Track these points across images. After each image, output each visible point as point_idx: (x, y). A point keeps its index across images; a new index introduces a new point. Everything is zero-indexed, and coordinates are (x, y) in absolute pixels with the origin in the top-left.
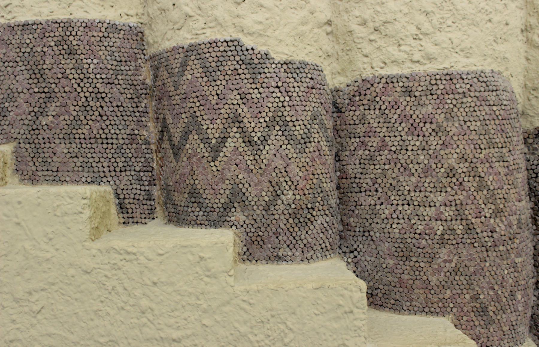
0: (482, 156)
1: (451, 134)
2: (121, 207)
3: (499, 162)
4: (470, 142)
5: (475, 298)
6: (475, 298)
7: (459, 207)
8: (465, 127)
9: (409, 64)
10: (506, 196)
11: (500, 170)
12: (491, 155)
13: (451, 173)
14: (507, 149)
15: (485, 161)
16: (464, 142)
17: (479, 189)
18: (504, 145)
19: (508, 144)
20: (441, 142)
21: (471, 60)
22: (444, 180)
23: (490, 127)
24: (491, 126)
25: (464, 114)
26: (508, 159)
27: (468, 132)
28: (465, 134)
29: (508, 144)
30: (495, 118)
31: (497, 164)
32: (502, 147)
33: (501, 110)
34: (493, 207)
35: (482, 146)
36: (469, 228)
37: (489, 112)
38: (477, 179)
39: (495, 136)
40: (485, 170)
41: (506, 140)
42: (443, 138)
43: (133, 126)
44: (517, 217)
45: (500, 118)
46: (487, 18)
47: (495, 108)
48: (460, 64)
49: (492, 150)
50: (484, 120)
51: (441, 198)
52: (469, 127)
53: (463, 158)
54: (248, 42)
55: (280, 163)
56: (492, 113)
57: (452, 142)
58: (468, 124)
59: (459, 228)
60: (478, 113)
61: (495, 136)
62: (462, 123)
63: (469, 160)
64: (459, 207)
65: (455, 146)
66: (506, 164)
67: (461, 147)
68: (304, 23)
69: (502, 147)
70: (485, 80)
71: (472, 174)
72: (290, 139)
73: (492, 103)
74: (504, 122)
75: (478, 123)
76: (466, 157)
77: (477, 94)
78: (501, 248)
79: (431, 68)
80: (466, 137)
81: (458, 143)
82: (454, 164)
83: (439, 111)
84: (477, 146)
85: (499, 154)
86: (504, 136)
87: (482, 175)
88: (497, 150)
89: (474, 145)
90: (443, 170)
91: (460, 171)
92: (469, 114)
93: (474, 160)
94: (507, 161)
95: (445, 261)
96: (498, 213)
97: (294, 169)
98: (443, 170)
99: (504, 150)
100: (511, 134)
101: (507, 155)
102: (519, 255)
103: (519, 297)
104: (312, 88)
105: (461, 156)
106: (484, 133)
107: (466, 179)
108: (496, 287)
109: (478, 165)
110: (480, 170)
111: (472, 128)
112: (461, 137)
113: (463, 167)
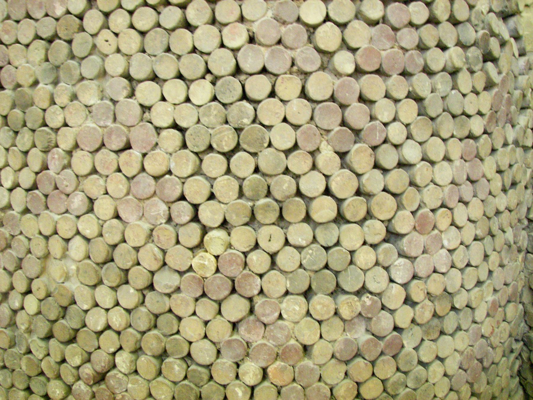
0: (204, 262)
1: (66, 140)
3: (308, 294)
4: (145, 184)
8: (130, 110)
11: (308, 334)
12: (258, 261)
14: (376, 230)
15: (219, 288)
16: (117, 185)
18: (355, 208)
19: (385, 206)
20: (26, 178)
22: (38, 348)
23: (270, 111)
24: (283, 114)
25: (131, 42)
26: (376, 281)
27: (141, 135)
28: (128, 147)
29: (385, 206)
30: (309, 60)
31: (294, 306)
32: (340, 219)
33: (358, 25)
35: (210, 214)
37: (267, 33)
38: (175, 368)
39: (299, 163)
40: (220, 330)
41: (374, 181)
42: (35, 159)
45: (345, 62)
49: (271, 237)
50: (238, 71)
52: (145, 108)
56: (293, 33)
57: (67, 180)
58: (147, 92)
60: (206, 37)
61: (299, 163)
62: (118, 87)
63: (139, 278)
65: (78, 202)
66: (348, 306)
67: (104, 207)
69: (340, 219)
71: (152, 342)
74: (373, 86)
75: (202, 91)
76: (123, 257)
80: (131, 161)
81: (94, 186)
82: (74, 286)
83: (26, 32)
84: (183, 212)
85: (314, 256)
87: (203, 352)
88: (300, 234)
89: (169, 204)
90: (31, 304)
91: (96, 320)
92: (156, 41)
93: (165, 281)
94: (362, 291)
98: (31, 304)
99: (352, 236)
100: (412, 153)
101: (366, 257)
105: (100, 252)
106: (228, 146)
107: (123, 361)
109: (182, 304)
110: (191, 329)
111: (162, 115)
112: (106, 159)
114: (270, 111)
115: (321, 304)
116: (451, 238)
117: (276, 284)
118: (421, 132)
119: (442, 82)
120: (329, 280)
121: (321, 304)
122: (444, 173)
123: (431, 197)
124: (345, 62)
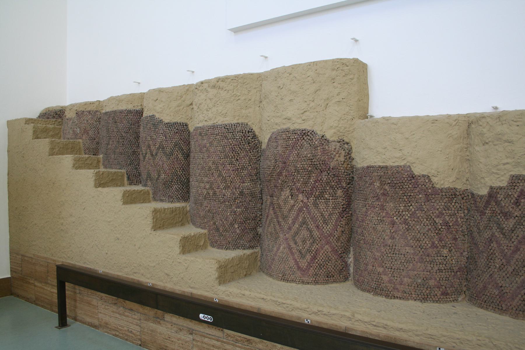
2: (129, 178)
5: (214, 223)
6: (214, 223)
7: (212, 184)
9: (204, 122)
10: (232, 180)
13: (210, 169)
14: (235, 159)
17: (219, 176)
18: (233, 157)
19: (236, 157)
21: (227, 119)
23: (226, 149)
26: (235, 164)
29: (236, 157)
34: (225, 185)
36: (215, 193)
41: (235, 155)
43: (134, 148)
44: (240, 190)
45: (233, 145)
46: (238, 98)
47: (230, 140)
48: (220, 120)
49: (226, 159)
51: (206, 179)
53: (214, 163)
54: (157, 116)
55: (161, 163)
59: (211, 193)
64: (212, 184)
66: (233, 166)
68: (178, 106)
70: (228, 127)
72: (165, 153)
73: (229, 138)
74: (235, 146)
77: (222, 134)
78: (227, 203)
79: (210, 123)
86: (234, 153)
88: (229, 159)
95: (206, 207)
96: (227, 187)
97: (165, 165)
99: (233, 159)
102: (238, 207)
103: (236, 226)
104: (177, 133)
108: (223, 220)
113: (213, 167)
114: (226, 149)
115: (230, 165)
116: (244, 160)
117: (227, 163)
118: (240, 150)
119: (243, 146)
120: (231, 163)
121: (230, 165)
122: (243, 154)
123: (241, 156)
124: (233, 145)
